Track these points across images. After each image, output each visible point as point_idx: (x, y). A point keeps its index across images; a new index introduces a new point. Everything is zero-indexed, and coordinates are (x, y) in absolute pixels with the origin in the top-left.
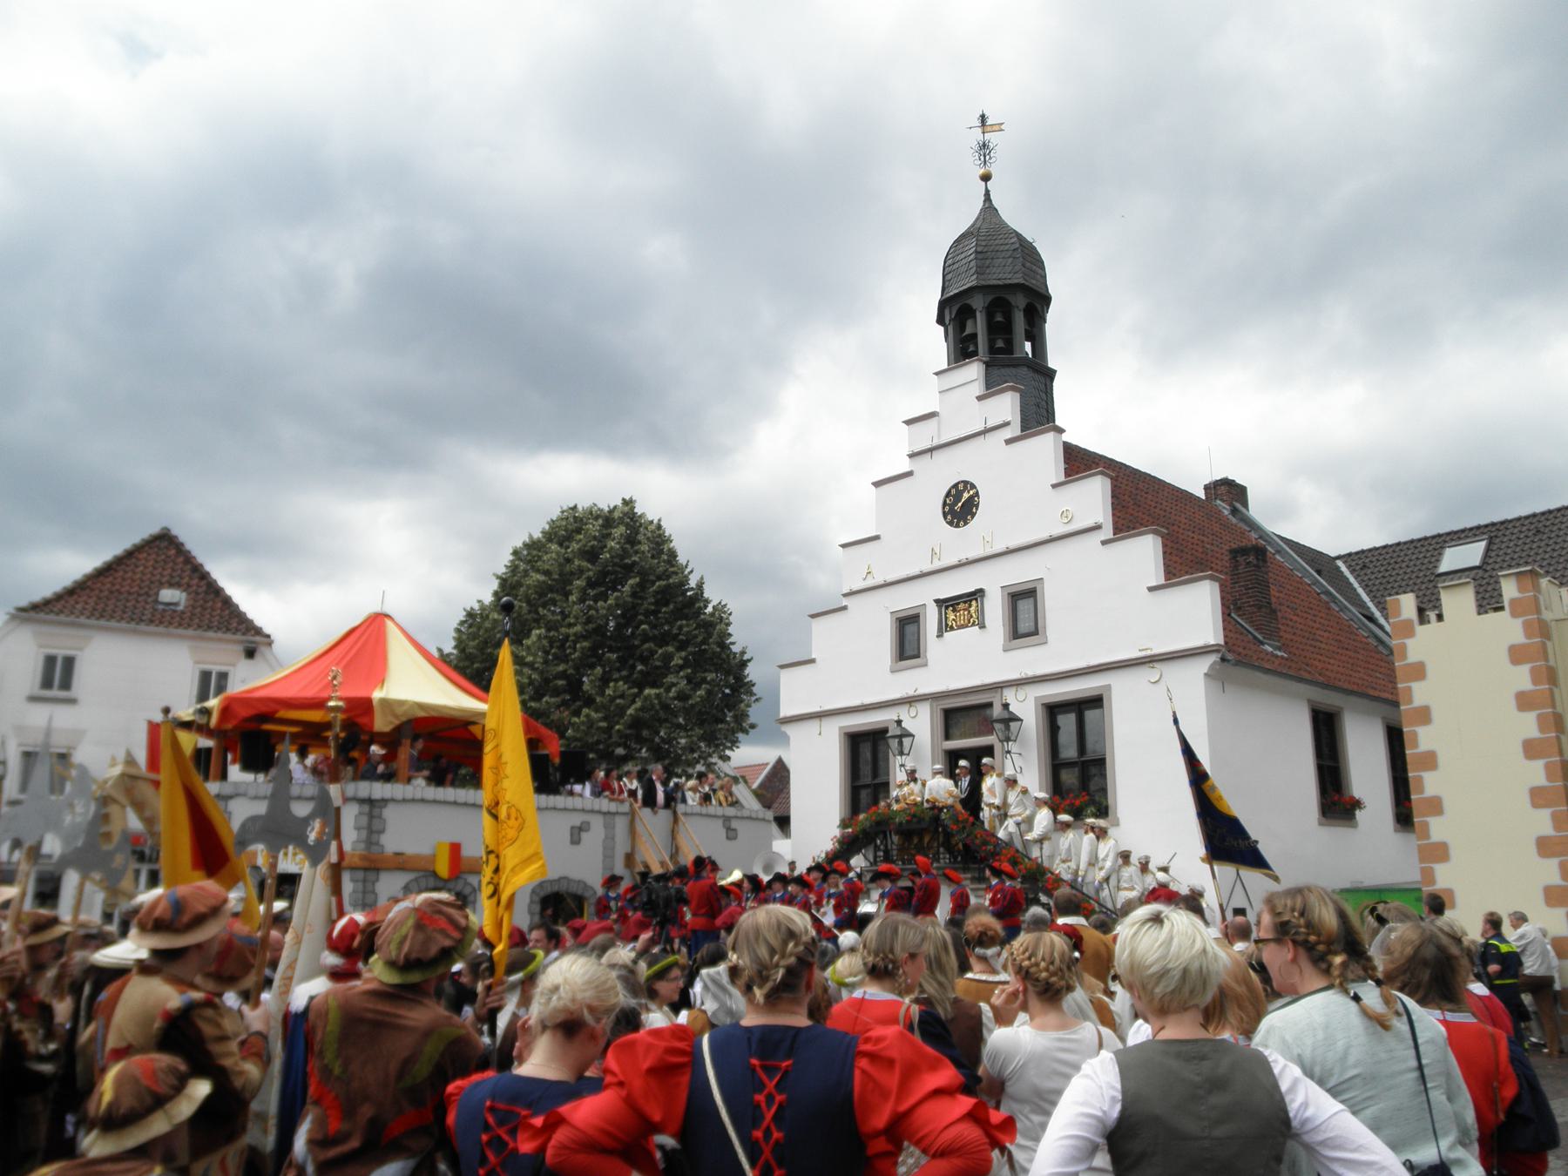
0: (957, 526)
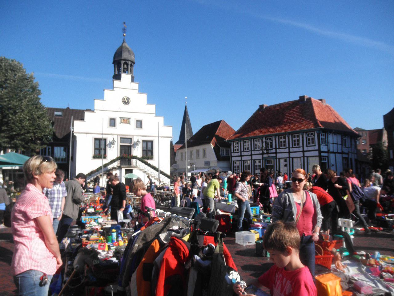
0: (125, 104)
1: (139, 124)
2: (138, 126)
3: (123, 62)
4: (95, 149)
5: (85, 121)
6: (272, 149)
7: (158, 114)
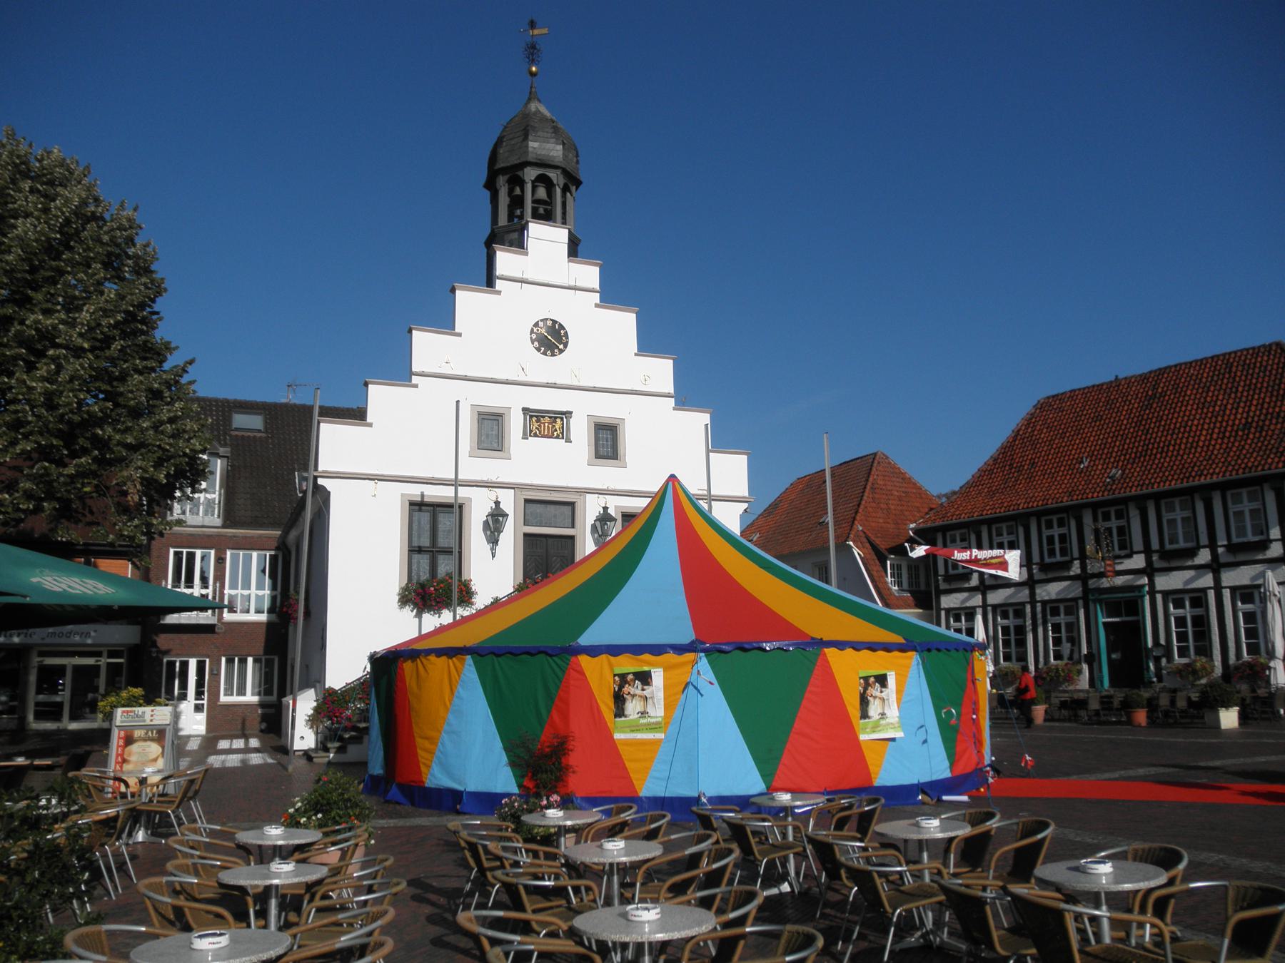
1: (607, 441)
2: (603, 451)
3: (530, 174)
4: (414, 550)
5: (370, 425)
6: (1129, 556)
7: (685, 397)
